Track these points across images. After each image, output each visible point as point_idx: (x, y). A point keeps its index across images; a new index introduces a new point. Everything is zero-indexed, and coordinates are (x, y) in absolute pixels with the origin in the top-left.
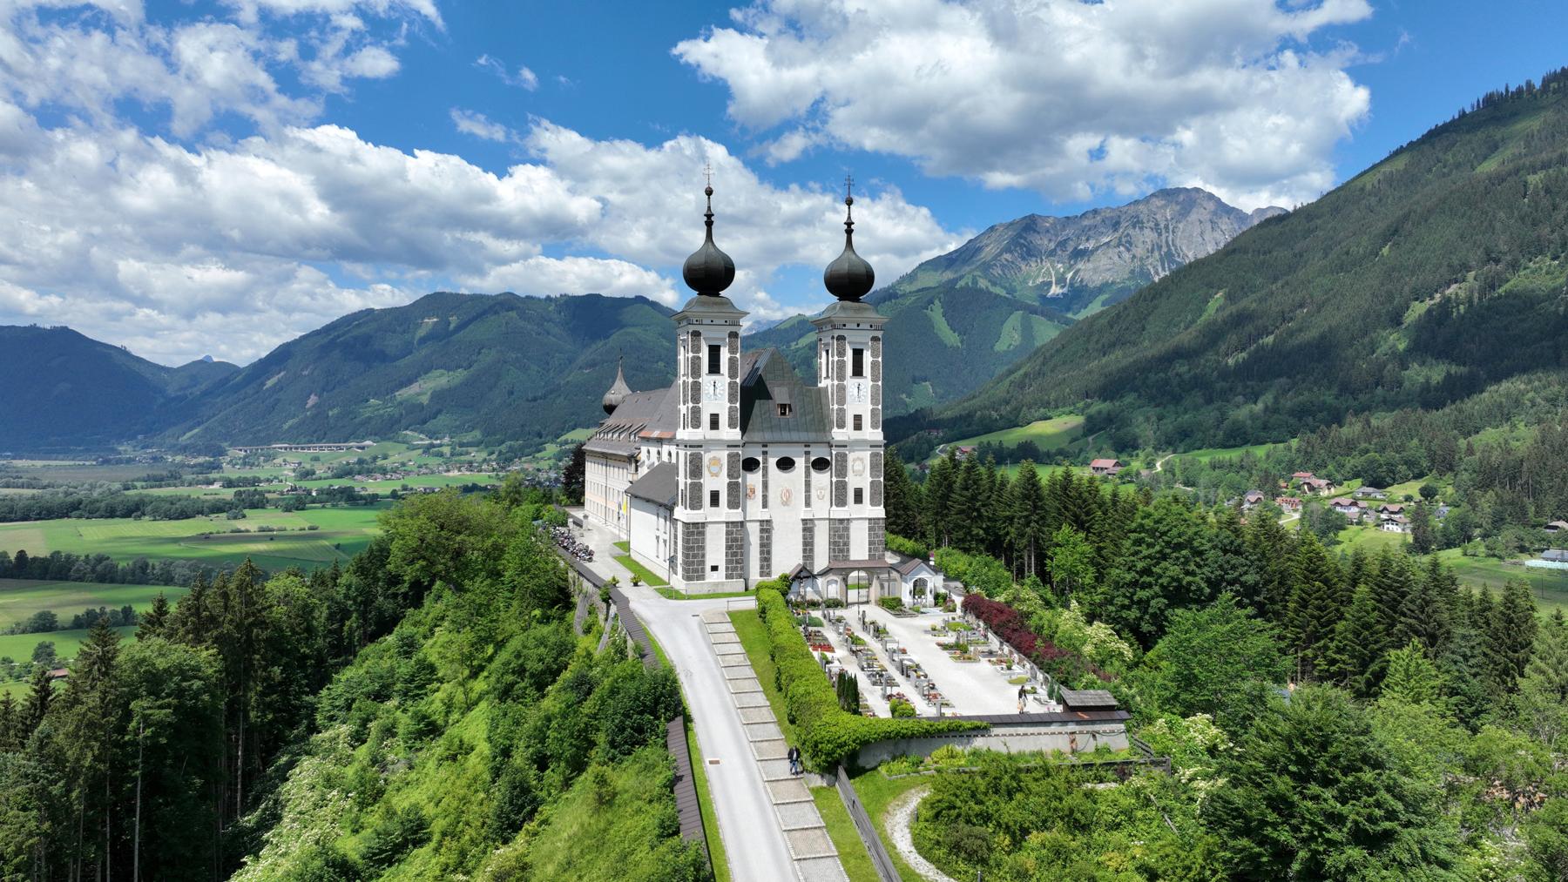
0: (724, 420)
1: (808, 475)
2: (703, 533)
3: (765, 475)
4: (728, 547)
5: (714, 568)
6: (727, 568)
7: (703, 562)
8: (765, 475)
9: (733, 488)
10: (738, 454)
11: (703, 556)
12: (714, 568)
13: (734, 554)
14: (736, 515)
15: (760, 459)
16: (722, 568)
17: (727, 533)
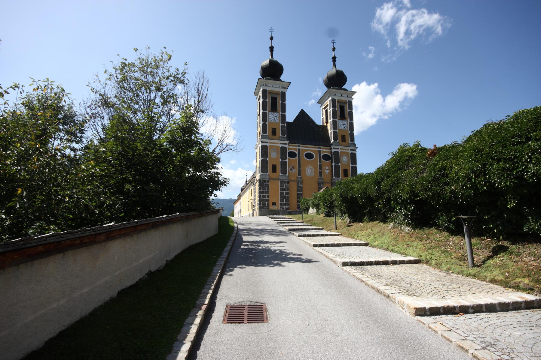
0: (279, 132)
1: (320, 161)
2: (268, 185)
3: (299, 160)
4: (281, 193)
5: (274, 204)
6: (281, 204)
7: (267, 200)
8: (299, 160)
9: (284, 164)
10: (286, 147)
11: (268, 197)
12: (274, 204)
13: (284, 197)
14: (285, 177)
15: (297, 153)
16: (278, 203)
17: (281, 186)
